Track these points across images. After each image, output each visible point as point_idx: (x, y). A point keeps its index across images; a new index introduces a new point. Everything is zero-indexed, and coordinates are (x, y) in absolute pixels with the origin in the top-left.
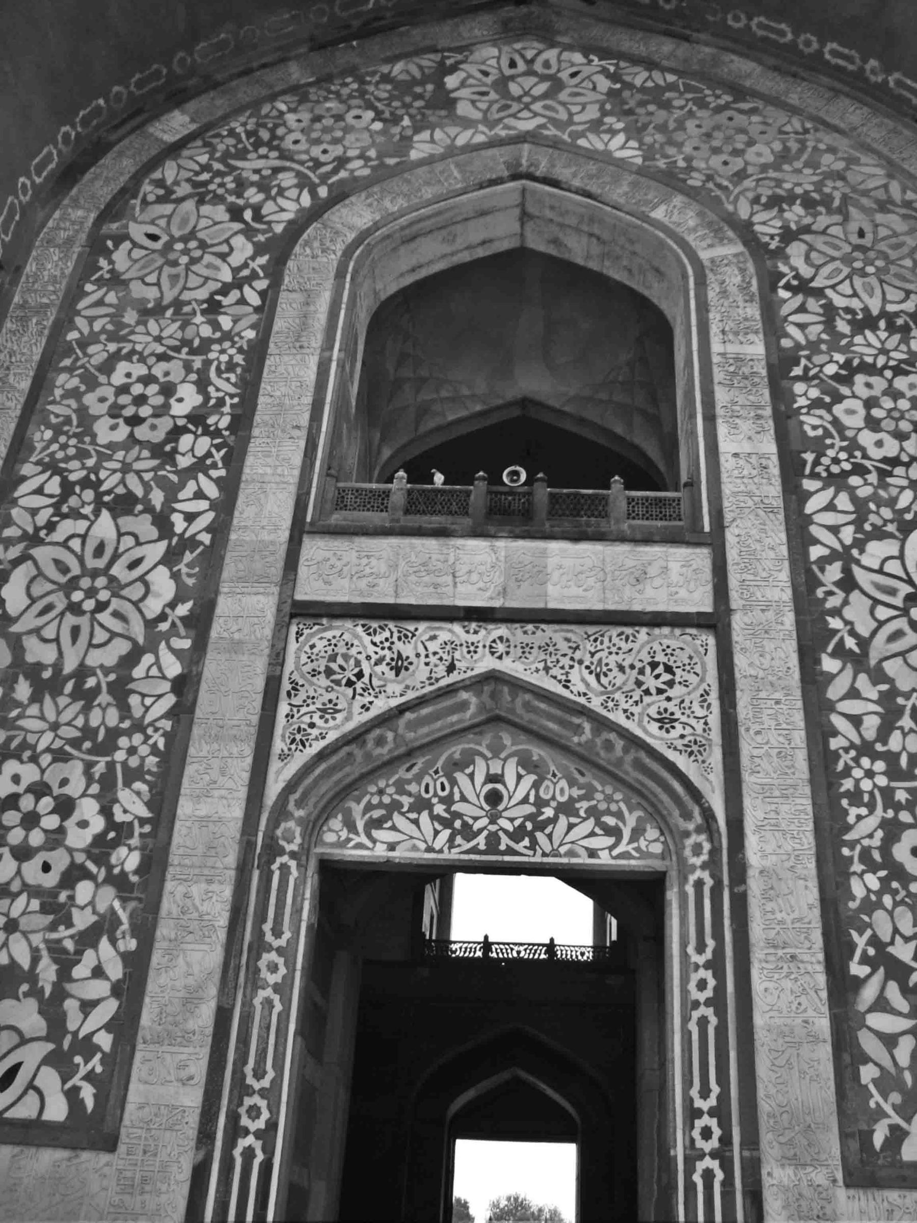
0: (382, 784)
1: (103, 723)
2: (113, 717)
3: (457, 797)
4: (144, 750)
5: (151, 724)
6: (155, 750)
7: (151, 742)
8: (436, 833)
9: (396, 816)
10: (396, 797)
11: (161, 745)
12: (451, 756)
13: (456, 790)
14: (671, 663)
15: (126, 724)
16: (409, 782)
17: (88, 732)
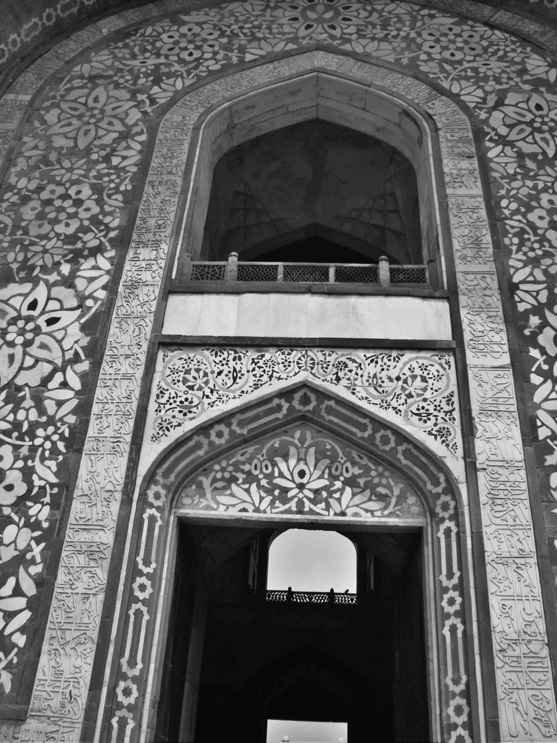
0: (224, 464)
1: (27, 418)
2: (33, 415)
3: (276, 474)
4: (55, 438)
5: (61, 420)
6: (62, 437)
7: (60, 431)
8: (262, 499)
9: (233, 486)
10: (233, 473)
11: (67, 434)
12: (272, 446)
13: (276, 470)
14: (425, 374)
15: (44, 419)
16: (243, 463)
17: (17, 425)
